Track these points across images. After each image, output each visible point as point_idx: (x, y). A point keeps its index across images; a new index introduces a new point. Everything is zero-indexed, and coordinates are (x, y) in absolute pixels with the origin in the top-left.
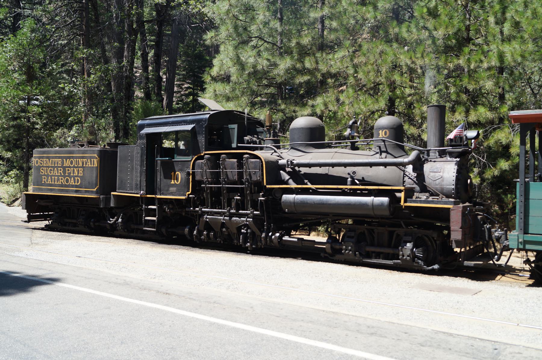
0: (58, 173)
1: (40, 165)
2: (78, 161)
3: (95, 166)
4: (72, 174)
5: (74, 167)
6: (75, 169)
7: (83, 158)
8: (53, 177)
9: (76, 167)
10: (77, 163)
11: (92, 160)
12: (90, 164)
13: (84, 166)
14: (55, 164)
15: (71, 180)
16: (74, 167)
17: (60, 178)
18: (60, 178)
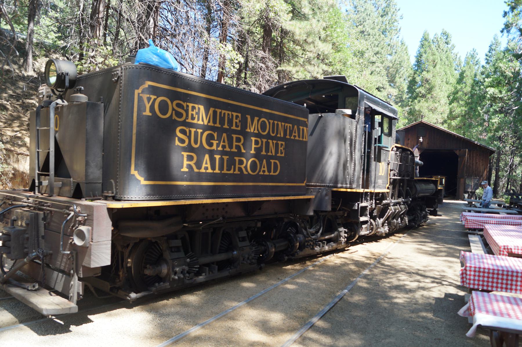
0: (231, 147)
1: (174, 117)
2: (278, 124)
3: (304, 140)
4: (264, 153)
5: (268, 137)
6: (270, 141)
7: (285, 120)
8: (217, 157)
9: (273, 138)
10: (274, 128)
11: (301, 128)
12: (297, 134)
13: (288, 137)
14: (222, 122)
15: (261, 164)
16: (268, 137)
17: (237, 159)
18: (237, 159)
